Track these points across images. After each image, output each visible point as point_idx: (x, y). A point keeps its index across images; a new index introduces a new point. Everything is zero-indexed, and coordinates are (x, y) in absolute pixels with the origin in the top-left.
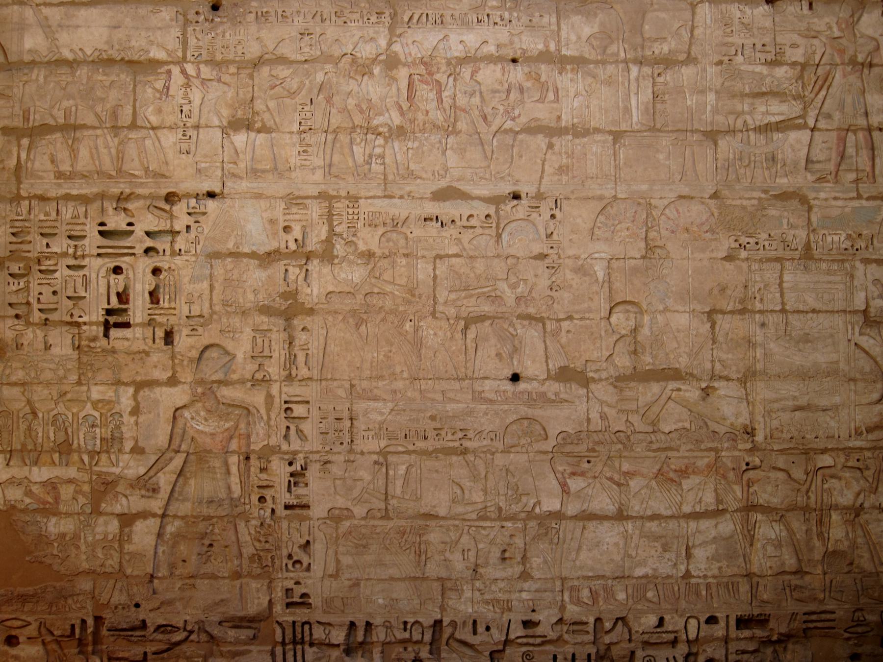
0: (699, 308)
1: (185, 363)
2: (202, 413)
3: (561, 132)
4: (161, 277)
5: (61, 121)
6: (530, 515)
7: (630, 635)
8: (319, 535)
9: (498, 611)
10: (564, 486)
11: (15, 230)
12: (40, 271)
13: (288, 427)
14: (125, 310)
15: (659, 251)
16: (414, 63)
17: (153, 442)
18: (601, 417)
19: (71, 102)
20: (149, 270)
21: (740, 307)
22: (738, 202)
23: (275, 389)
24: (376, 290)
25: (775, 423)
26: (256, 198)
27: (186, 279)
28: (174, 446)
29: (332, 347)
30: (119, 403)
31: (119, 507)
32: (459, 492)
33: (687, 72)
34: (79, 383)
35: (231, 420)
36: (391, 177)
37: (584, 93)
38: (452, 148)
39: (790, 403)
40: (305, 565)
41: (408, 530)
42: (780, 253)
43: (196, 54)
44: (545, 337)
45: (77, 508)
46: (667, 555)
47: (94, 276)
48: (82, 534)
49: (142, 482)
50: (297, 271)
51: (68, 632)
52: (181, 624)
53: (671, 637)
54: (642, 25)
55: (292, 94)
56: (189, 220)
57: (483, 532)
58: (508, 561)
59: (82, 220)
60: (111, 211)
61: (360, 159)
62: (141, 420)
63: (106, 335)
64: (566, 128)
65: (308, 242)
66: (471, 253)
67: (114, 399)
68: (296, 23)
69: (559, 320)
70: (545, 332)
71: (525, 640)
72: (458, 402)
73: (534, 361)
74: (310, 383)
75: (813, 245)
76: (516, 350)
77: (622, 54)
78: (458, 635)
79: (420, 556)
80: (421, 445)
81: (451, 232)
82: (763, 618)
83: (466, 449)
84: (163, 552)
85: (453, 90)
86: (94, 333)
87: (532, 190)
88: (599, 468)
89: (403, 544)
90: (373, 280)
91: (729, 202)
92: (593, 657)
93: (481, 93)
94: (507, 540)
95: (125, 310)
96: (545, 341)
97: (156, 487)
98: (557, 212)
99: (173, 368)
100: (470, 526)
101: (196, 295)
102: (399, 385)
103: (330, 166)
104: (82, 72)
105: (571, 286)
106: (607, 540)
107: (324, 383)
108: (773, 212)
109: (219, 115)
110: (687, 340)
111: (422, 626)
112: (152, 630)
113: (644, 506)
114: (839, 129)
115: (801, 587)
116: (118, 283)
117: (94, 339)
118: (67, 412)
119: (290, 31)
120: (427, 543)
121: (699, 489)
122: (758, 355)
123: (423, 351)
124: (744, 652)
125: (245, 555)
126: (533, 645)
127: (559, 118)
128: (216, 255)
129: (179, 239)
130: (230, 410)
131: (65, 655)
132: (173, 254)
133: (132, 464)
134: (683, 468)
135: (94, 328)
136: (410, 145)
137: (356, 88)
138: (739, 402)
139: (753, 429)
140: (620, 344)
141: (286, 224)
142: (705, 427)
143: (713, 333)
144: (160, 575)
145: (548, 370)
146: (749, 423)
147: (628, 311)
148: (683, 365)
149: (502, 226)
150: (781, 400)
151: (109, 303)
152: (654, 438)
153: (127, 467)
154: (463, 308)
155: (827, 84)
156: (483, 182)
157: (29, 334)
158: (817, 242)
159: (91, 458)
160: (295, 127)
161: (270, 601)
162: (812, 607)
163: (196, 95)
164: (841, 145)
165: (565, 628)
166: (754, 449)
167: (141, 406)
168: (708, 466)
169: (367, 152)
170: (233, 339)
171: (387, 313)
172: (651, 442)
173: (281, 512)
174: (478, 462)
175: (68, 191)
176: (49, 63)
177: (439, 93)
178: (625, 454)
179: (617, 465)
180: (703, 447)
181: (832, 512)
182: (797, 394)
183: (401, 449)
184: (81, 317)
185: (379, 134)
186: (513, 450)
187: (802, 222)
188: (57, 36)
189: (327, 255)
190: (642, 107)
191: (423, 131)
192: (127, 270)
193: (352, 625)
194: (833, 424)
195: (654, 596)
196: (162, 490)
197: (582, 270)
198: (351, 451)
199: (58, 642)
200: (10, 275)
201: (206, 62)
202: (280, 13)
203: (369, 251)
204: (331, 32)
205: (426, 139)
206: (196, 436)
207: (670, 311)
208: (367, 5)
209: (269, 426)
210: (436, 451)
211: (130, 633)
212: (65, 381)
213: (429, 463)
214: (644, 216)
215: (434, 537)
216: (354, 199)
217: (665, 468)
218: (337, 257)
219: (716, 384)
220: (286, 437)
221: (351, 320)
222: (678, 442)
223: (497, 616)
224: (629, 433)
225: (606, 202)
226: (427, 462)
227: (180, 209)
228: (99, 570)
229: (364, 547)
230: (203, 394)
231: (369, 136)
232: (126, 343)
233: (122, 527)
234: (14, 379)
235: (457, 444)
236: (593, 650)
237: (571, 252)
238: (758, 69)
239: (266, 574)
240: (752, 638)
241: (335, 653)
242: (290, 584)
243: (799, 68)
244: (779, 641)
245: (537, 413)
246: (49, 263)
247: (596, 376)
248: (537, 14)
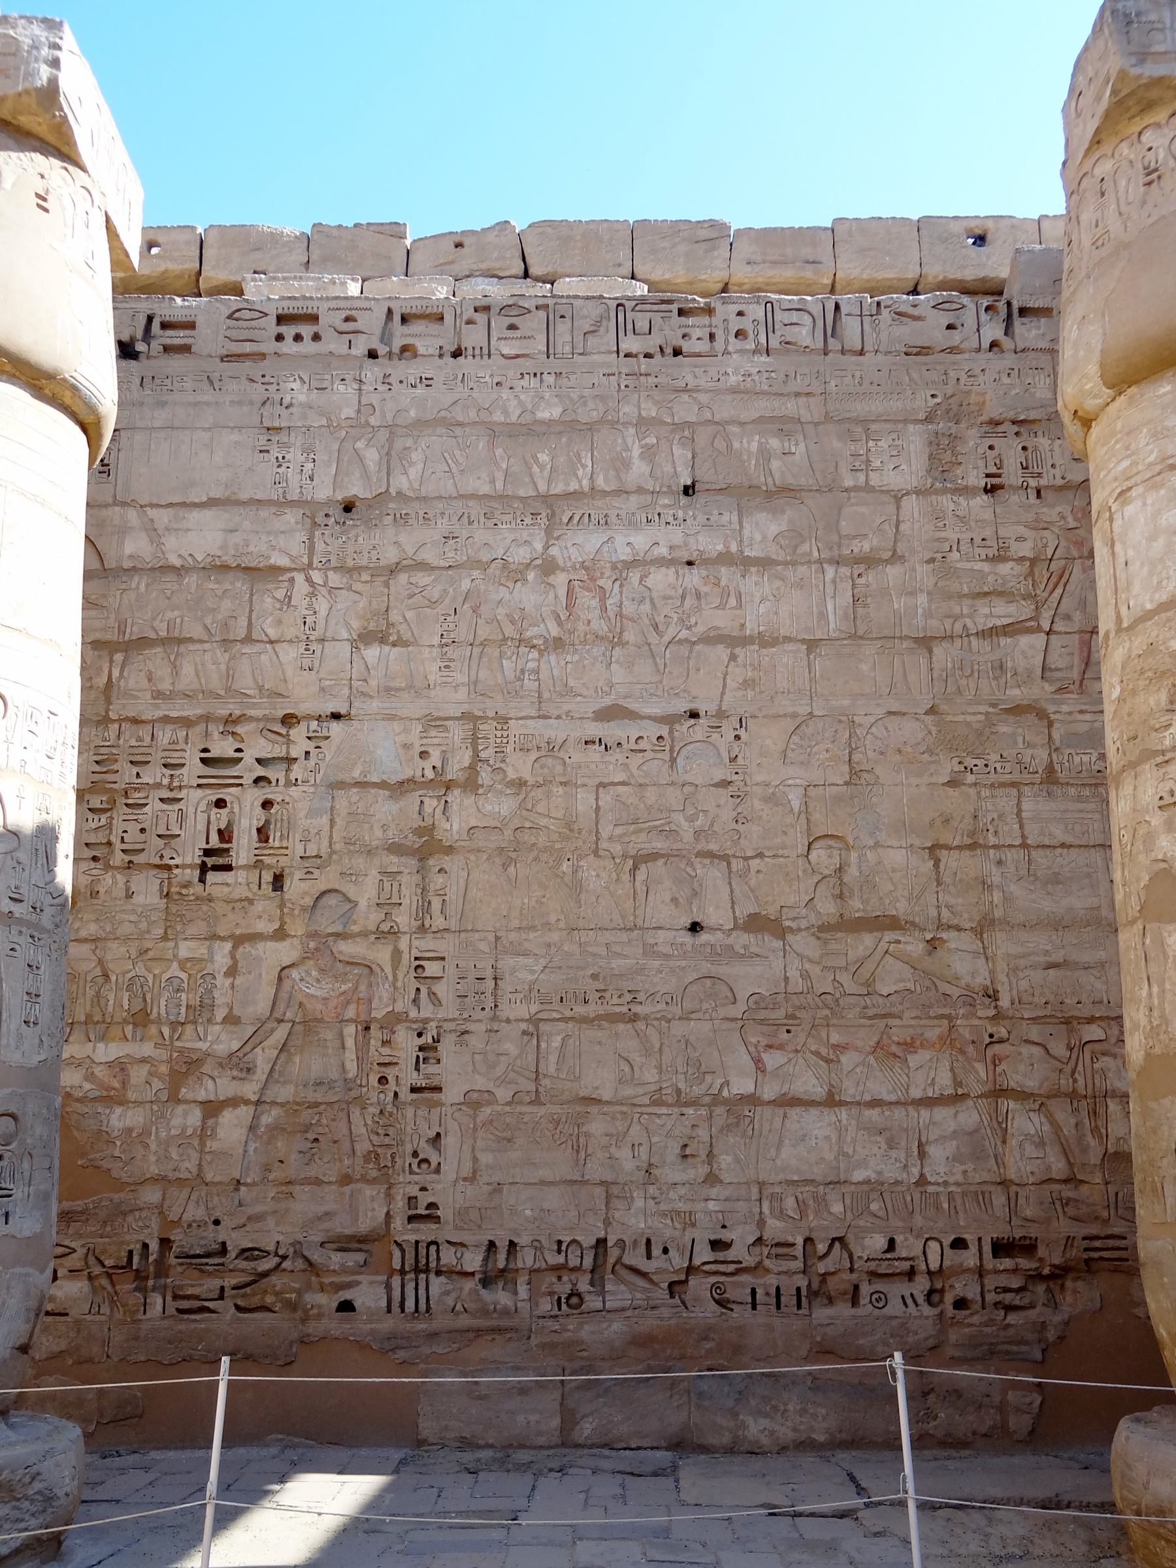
0: (917, 842)
1: (296, 912)
2: (314, 973)
3: (745, 641)
4: (272, 811)
5: (163, 634)
6: (717, 1100)
7: (851, 1262)
8: (452, 1126)
9: (678, 1226)
10: (758, 1062)
11: (99, 758)
12: (126, 805)
13: (418, 989)
14: (227, 850)
15: (865, 775)
16: (574, 568)
17: (251, 1009)
18: (801, 975)
19: (176, 613)
20: (258, 803)
21: (969, 841)
22: (961, 718)
23: (403, 944)
24: (527, 825)
25: (1024, 984)
26: (389, 719)
27: (302, 814)
28: (277, 1015)
29: (474, 892)
30: (212, 962)
31: (203, 1092)
32: (627, 1069)
33: (893, 573)
34: (165, 938)
35: (349, 981)
36: (546, 695)
37: (772, 598)
38: (617, 662)
39: (1042, 959)
40: (434, 1165)
41: (564, 1119)
42: (1016, 777)
43: (324, 560)
44: (730, 878)
45: (149, 1096)
46: (894, 1154)
47: (191, 810)
48: (154, 1129)
49: (234, 1059)
50: (435, 802)
51: (124, 1262)
52: (271, 1248)
53: (906, 1266)
54: (838, 522)
55: (433, 604)
56: (310, 746)
57: (658, 1121)
58: (690, 1160)
59: (182, 746)
60: (216, 735)
61: (510, 675)
62: (238, 982)
63: (202, 880)
64: (751, 637)
65: (448, 769)
66: (641, 781)
67: (206, 957)
68: (439, 525)
69: (746, 859)
70: (730, 872)
71: (713, 1267)
72: (626, 957)
73: (717, 907)
74: (446, 935)
75: (1057, 767)
76: (695, 894)
77: (816, 554)
78: (627, 1260)
79: (578, 1152)
80: (580, 1010)
81: (617, 756)
82: (1028, 1242)
83: (635, 1014)
84: (256, 1150)
85: (618, 597)
86: (187, 878)
87: (712, 708)
88: (801, 1039)
89: (557, 1136)
90: (525, 813)
91: (949, 718)
92: (804, 1292)
93: (652, 599)
94: (688, 1131)
95: (227, 850)
96: (730, 883)
97: (251, 1066)
98: (742, 733)
99: (281, 919)
100: (642, 1114)
101: (313, 831)
102: (555, 936)
103: (475, 683)
104: (191, 580)
105: (760, 818)
106: (816, 1132)
107: (463, 935)
108: (1004, 729)
109: (348, 626)
110: (905, 881)
111: (581, 1247)
112: (233, 1255)
113: (861, 1088)
114: (1081, 632)
115: (1077, 1201)
116: (220, 818)
117: (187, 885)
118: (146, 974)
119: (434, 534)
120: (588, 1135)
121: (930, 1068)
122: (995, 899)
123: (583, 897)
124: (1006, 1290)
125: (358, 1153)
126: (724, 1274)
127: (743, 625)
128: (341, 785)
129: (295, 767)
130: (348, 968)
131: (116, 1292)
132: (288, 784)
133: (223, 1037)
134: (909, 1040)
135: (188, 871)
136: (569, 658)
137: (507, 596)
138: (974, 957)
139: (996, 991)
140: (822, 888)
141: (423, 749)
142: (933, 988)
143: (938, 873)
144: (249, 1180)
145: (735, 918)
146: (988, 982)
147: (831, 847)
148: (902, 911)
149: (677, 749)
150: (1029, 955)
151: (208, 843)
152: (868, 1002)
153: (217, 1040)
154: (632, 844)
155: (1064, 580)
156: (655, 699)
157: (108, 879)
158: (1062, 764)
159: (174, 1030)
160: (436, 640)
161: (388, 1213)
162: (1094, 1230)
164: (1085, 649)
165: (766, 1251)
166: (998, 1017)
167: (239, 965)
168: (940, 1037)
169: (519, 667)
170: (355, 883)
171: (541, 851)
172: (865, 1008)
173: (405, 1095)
174: (651, 1031)
175: (167, 713)
176: (153, 569)
177: (603, 600)
178: (834, 1021)
179: (824, 1035)
180: (932, 1014)
181: (1108, 1100)
182: (1049, 948)
183: (555, 1015)
184: (172, 858)
185: (534, 647)
186: (693, 1016)
187: (1042, 739)
188: (163, 540)
189: (471, 784)
190: (840, 612)
191: (584, 642)
192: (232, 803)
193: (492, 1245)
194: (1099, 985)
195: (880, 1209)
196: (259, 1071)
197: (771, 799)
198: (495, 1018)
199: (109, 1276)
200: (90, 809)
201: (335, 569)
202: (421, 513)
203: (520, 779)
204: (481, 535)
205: (588, 651)
206: (304, 1001)
207: (882, 846)
208: (521, 506)
209: (395, 988)
210: (599, 1017)
211: (204, 1261)
212: (147, 936)
213: (590, 1033)
214: (847, 736)
215: (597, 1127)
216: (503, 720)
217: (885, 1041)
218: (482, 786)
219: (944, 935)
220: (415, 1001)
221: (497, 860)
222: (900, 1008)
223: (677, 1233)
224: (838, 995)
225: (798, 721)
226: (588, 1032)
227: (298, 733)
228: (170, 1174)
229: (509, 1141)
230: (317, 949)
231: (522, 649)
232: (226, 890)
233: (205, 1119)
234: (83, 934)
235: (624, 1009)
236: (802, 1282)
237: (759, 778)
238: (978, 566)
239: (385, 1179)
240: (1015, 1271)
241: (469, 1285)
242: (414, 1191)
243: (1028, 563)
244: (1052, 1277)
245: (722, 970)
246: (138, 795)
247: (794, 925)
248: (716, 512)
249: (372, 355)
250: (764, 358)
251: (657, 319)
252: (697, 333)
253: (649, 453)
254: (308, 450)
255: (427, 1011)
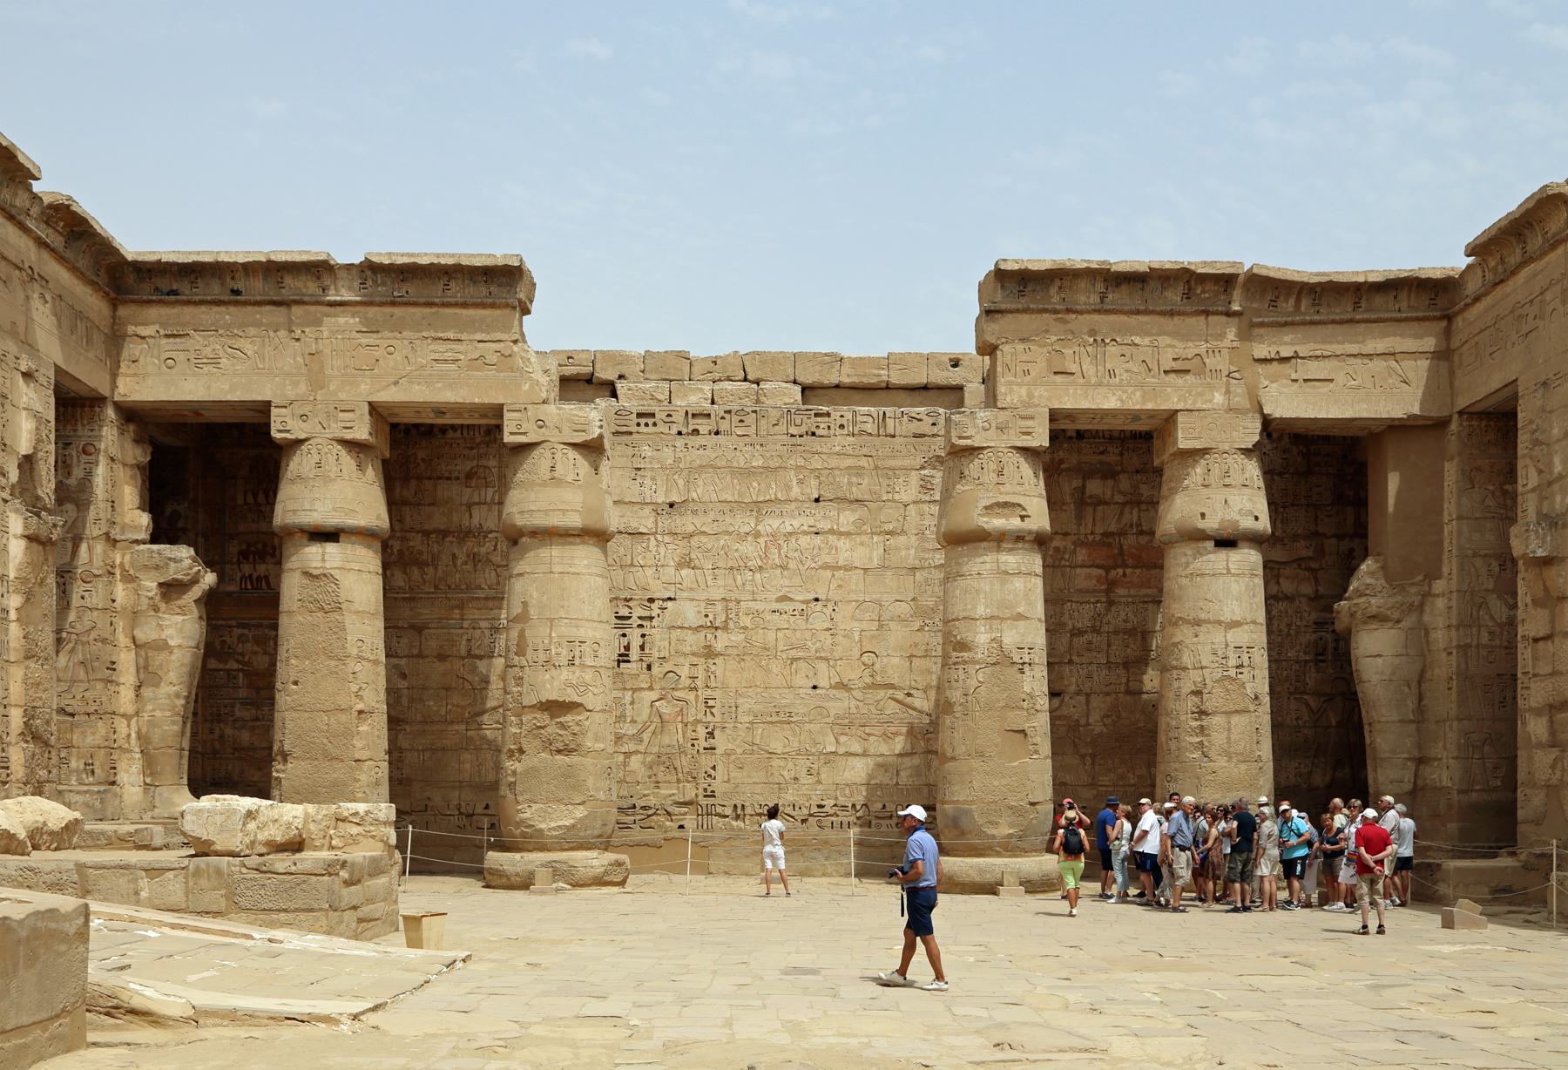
3: (840, 568)
6: (821, 753)
8: (720, 762)
33: (902, 539)
63: (619, 666)
80: (769, 719)
81: (784, 616)
116: (624, 641)
132: (651, 627)
160: (710, 567)
163: (662, 550)
173: (701, 750)
189: (725, 628)
204: (728, 520)
210: (777, 722)
213: (773, 728)
216: (739, 602)
227: (655, 606)
249: (680, 433)
250: (851, 439)
251: (805, 418)
252: (822, 426)
253: (800, 482)
254: (653, 479)
255: (710, 718)
